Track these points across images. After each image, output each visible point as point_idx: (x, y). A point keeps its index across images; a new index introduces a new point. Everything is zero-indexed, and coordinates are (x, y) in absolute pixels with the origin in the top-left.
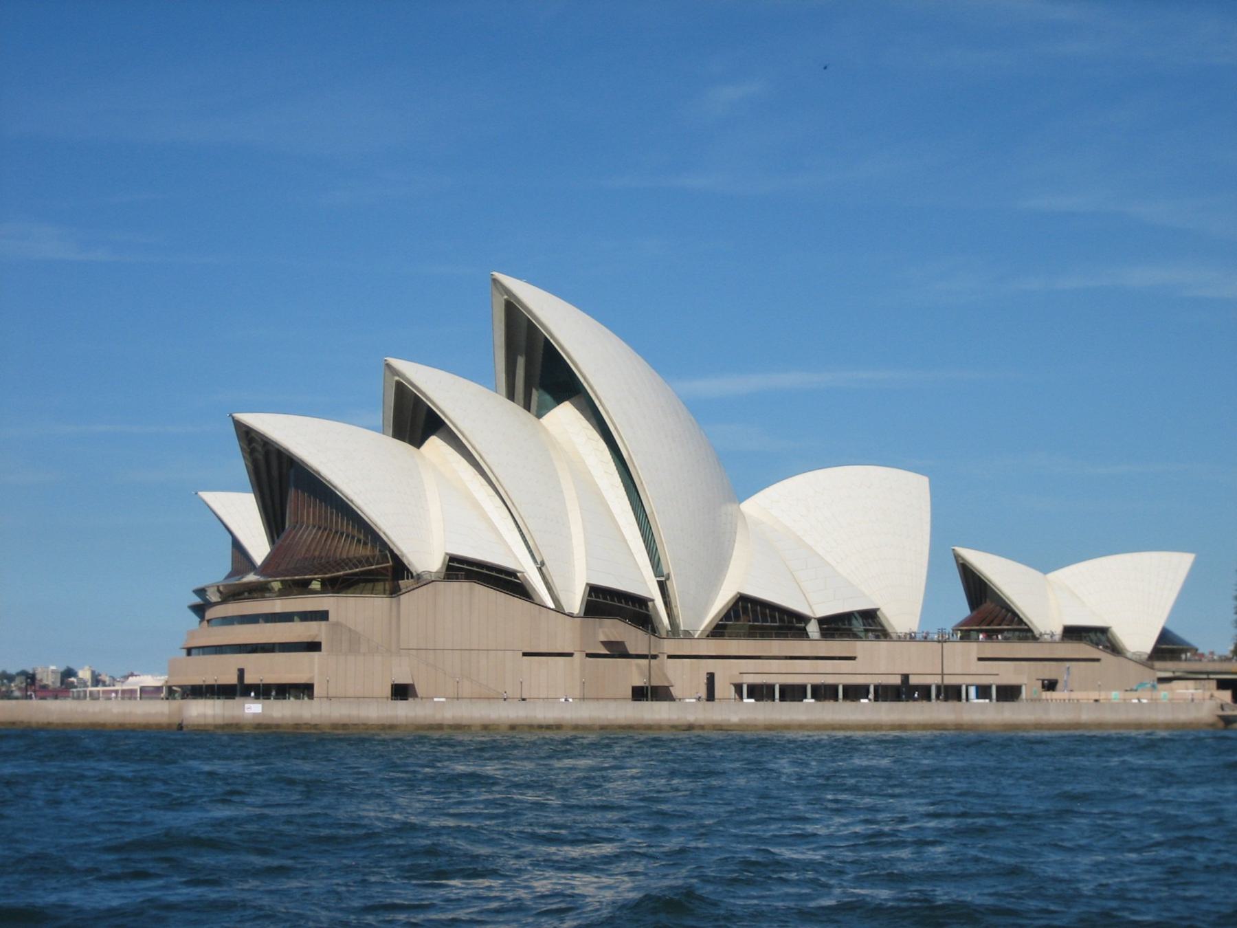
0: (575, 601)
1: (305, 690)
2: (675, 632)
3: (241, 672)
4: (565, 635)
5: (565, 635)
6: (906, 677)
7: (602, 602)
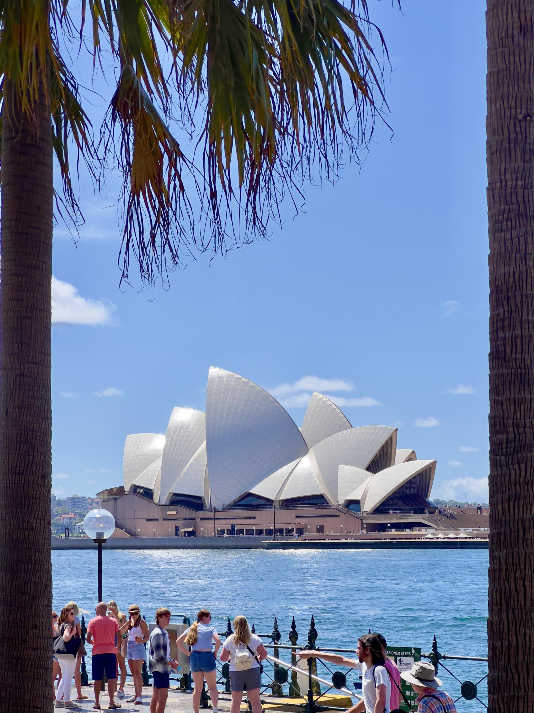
6: (233, 526)
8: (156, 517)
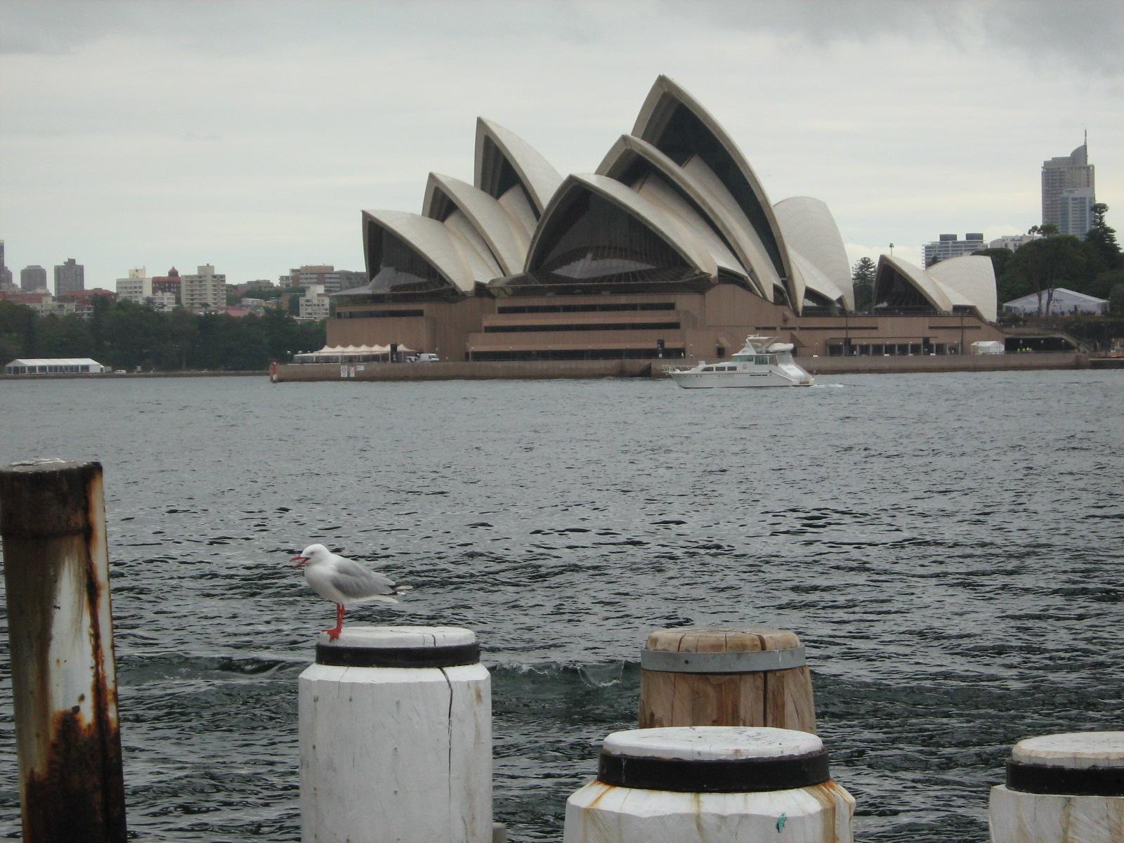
0: (770, 295)
2: (797, 314)
3: (661, 343)
4: (774, 316)
8: (774, 326)
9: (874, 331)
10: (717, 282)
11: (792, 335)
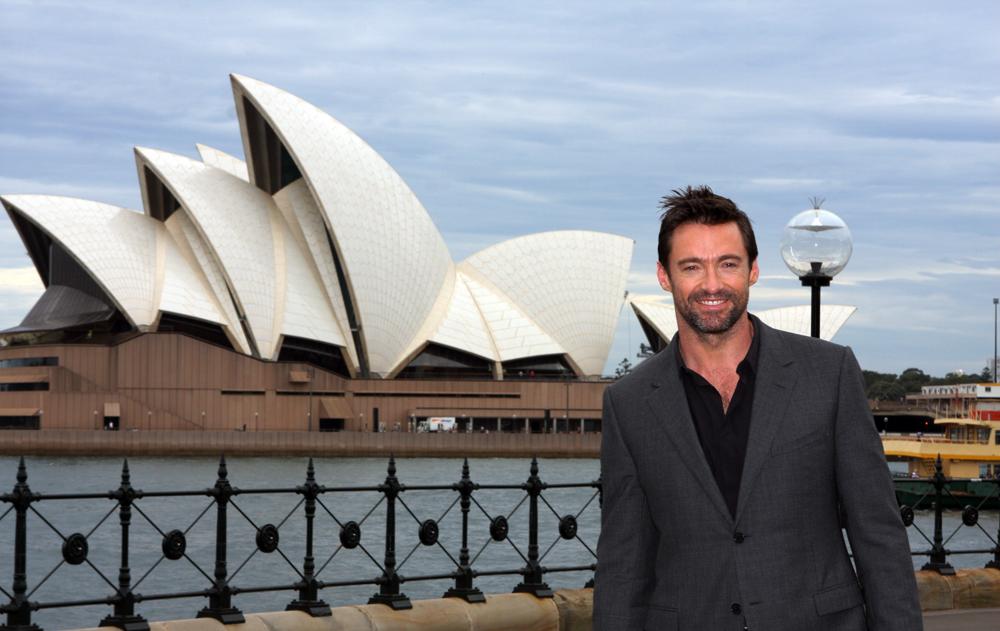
0: (268, 349)
1: (31, 422)
2: (365, 372)
5: (255, 379)
6: (548, 412)
7: (294, 349)
8: (262, 390)
9: (517, 400)
10: (154, 331)
11: (321, 405)
